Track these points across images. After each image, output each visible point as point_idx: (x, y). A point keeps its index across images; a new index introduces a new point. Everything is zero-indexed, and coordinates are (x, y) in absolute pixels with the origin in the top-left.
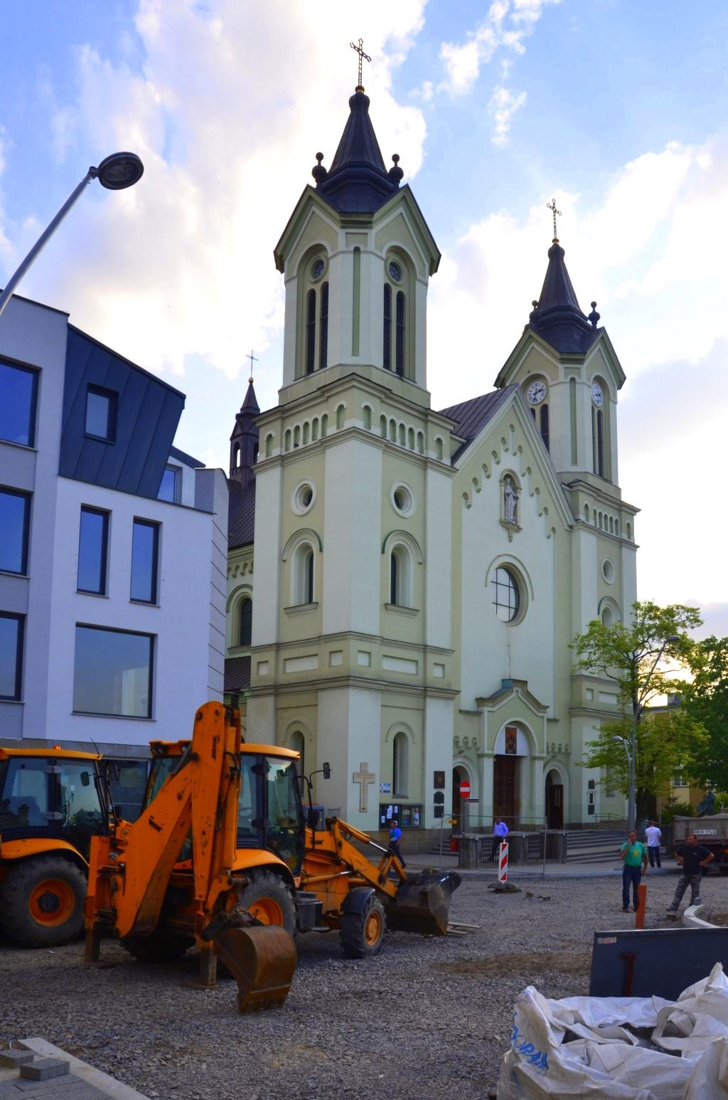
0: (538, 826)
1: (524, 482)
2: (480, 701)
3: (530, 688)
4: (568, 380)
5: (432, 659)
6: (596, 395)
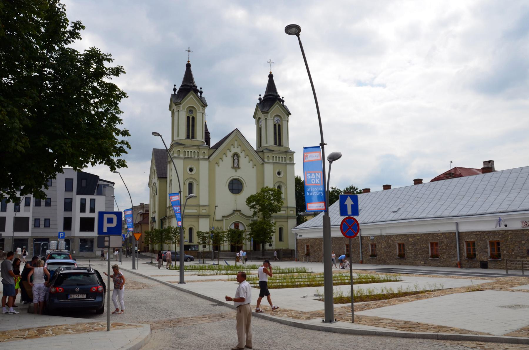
0: (248, 250)
2: (224, 217)
3: (243, 212)
4: (265, 119)
5: (201, 208)
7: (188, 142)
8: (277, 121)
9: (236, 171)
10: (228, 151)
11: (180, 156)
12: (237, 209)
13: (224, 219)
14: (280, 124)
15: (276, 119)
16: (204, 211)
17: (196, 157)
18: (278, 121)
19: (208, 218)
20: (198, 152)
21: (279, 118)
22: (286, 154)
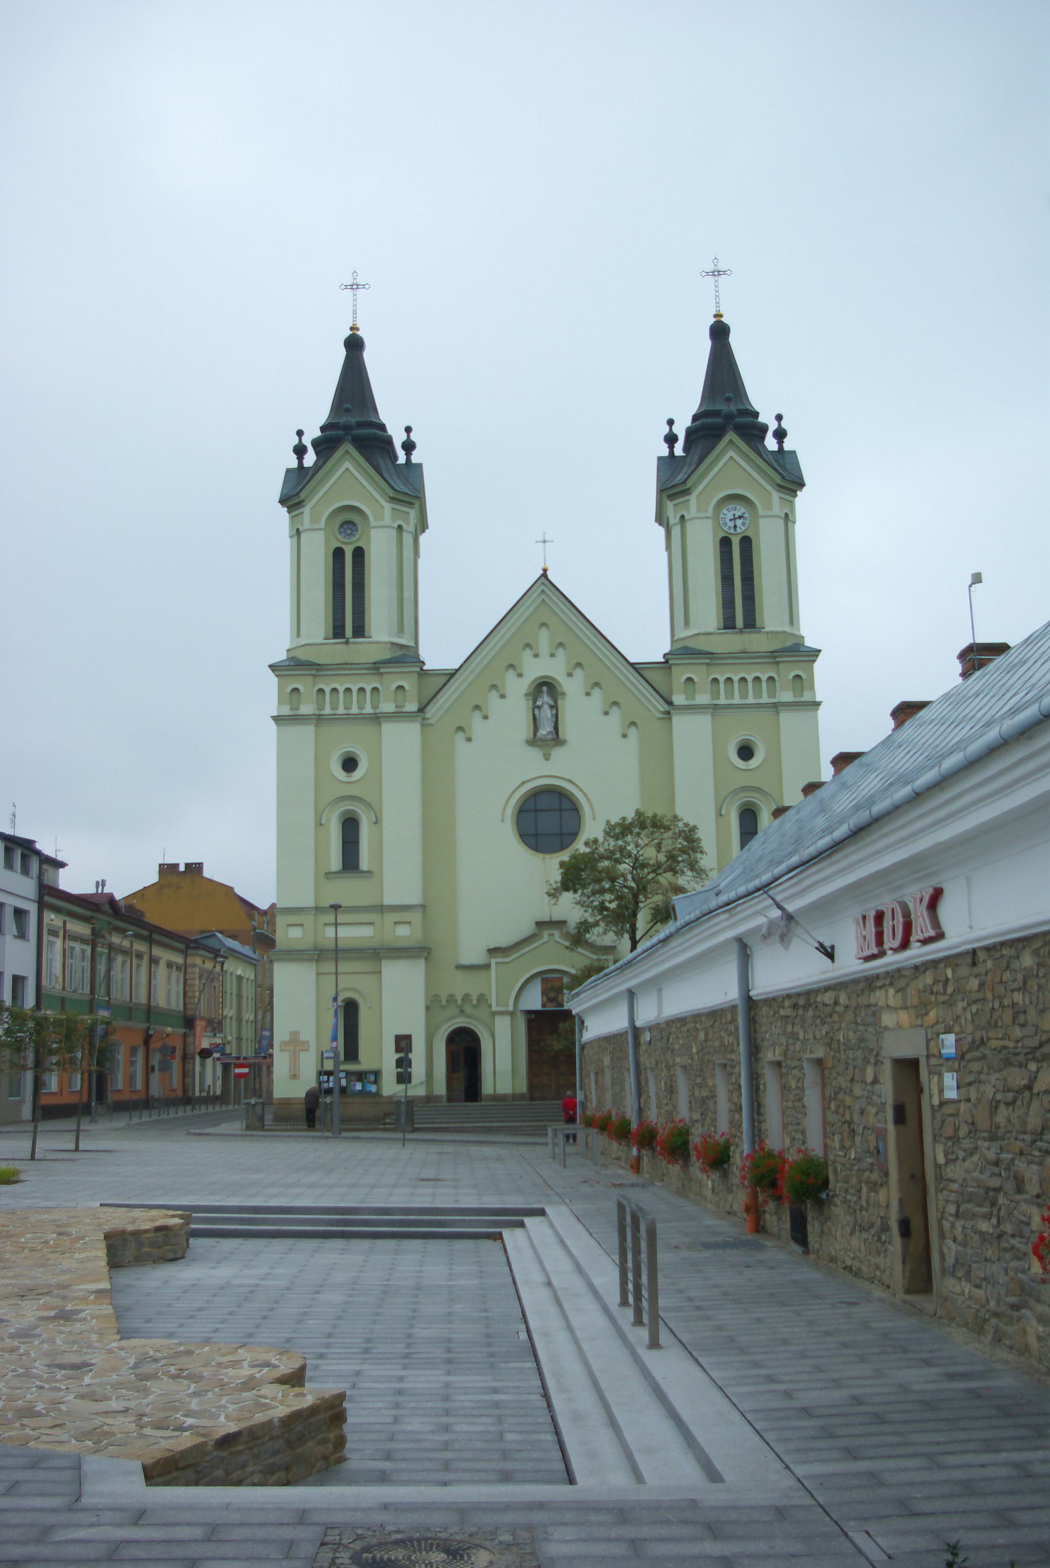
1: (566, 684)
2: (493, 951)
5: (390, 918)
6: (731, 520)
7: (338, 652)
8: (732, 524)
9: (547, 757)
10: (511, 675)
11: (300, 712)
12: (554, 919)
13: (493, 961)
14: (748, 534)
15: (730, 516)
16: (403, 931)
17: (368, 709)
18: (739, 522)
19: (418, 957)
20: (375, 689)
21: (740, 510)
22: (778, 663)
